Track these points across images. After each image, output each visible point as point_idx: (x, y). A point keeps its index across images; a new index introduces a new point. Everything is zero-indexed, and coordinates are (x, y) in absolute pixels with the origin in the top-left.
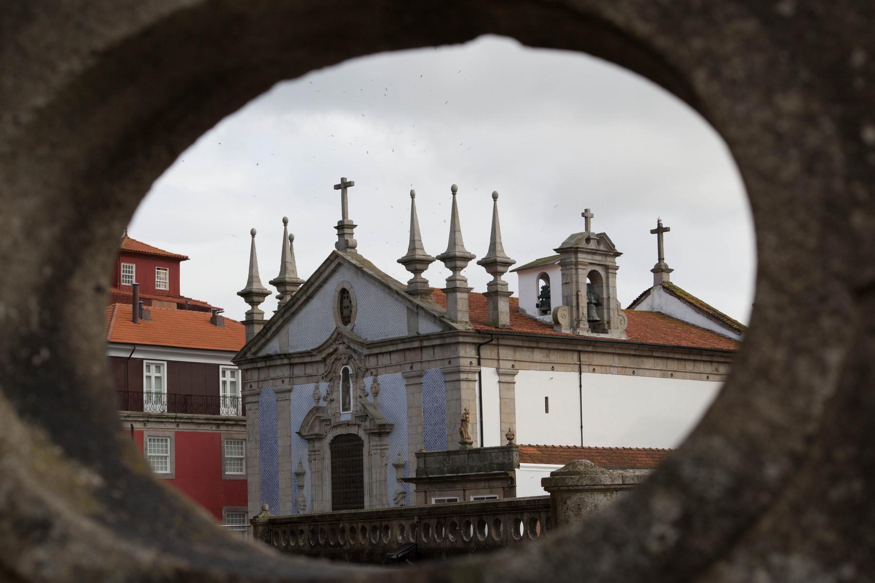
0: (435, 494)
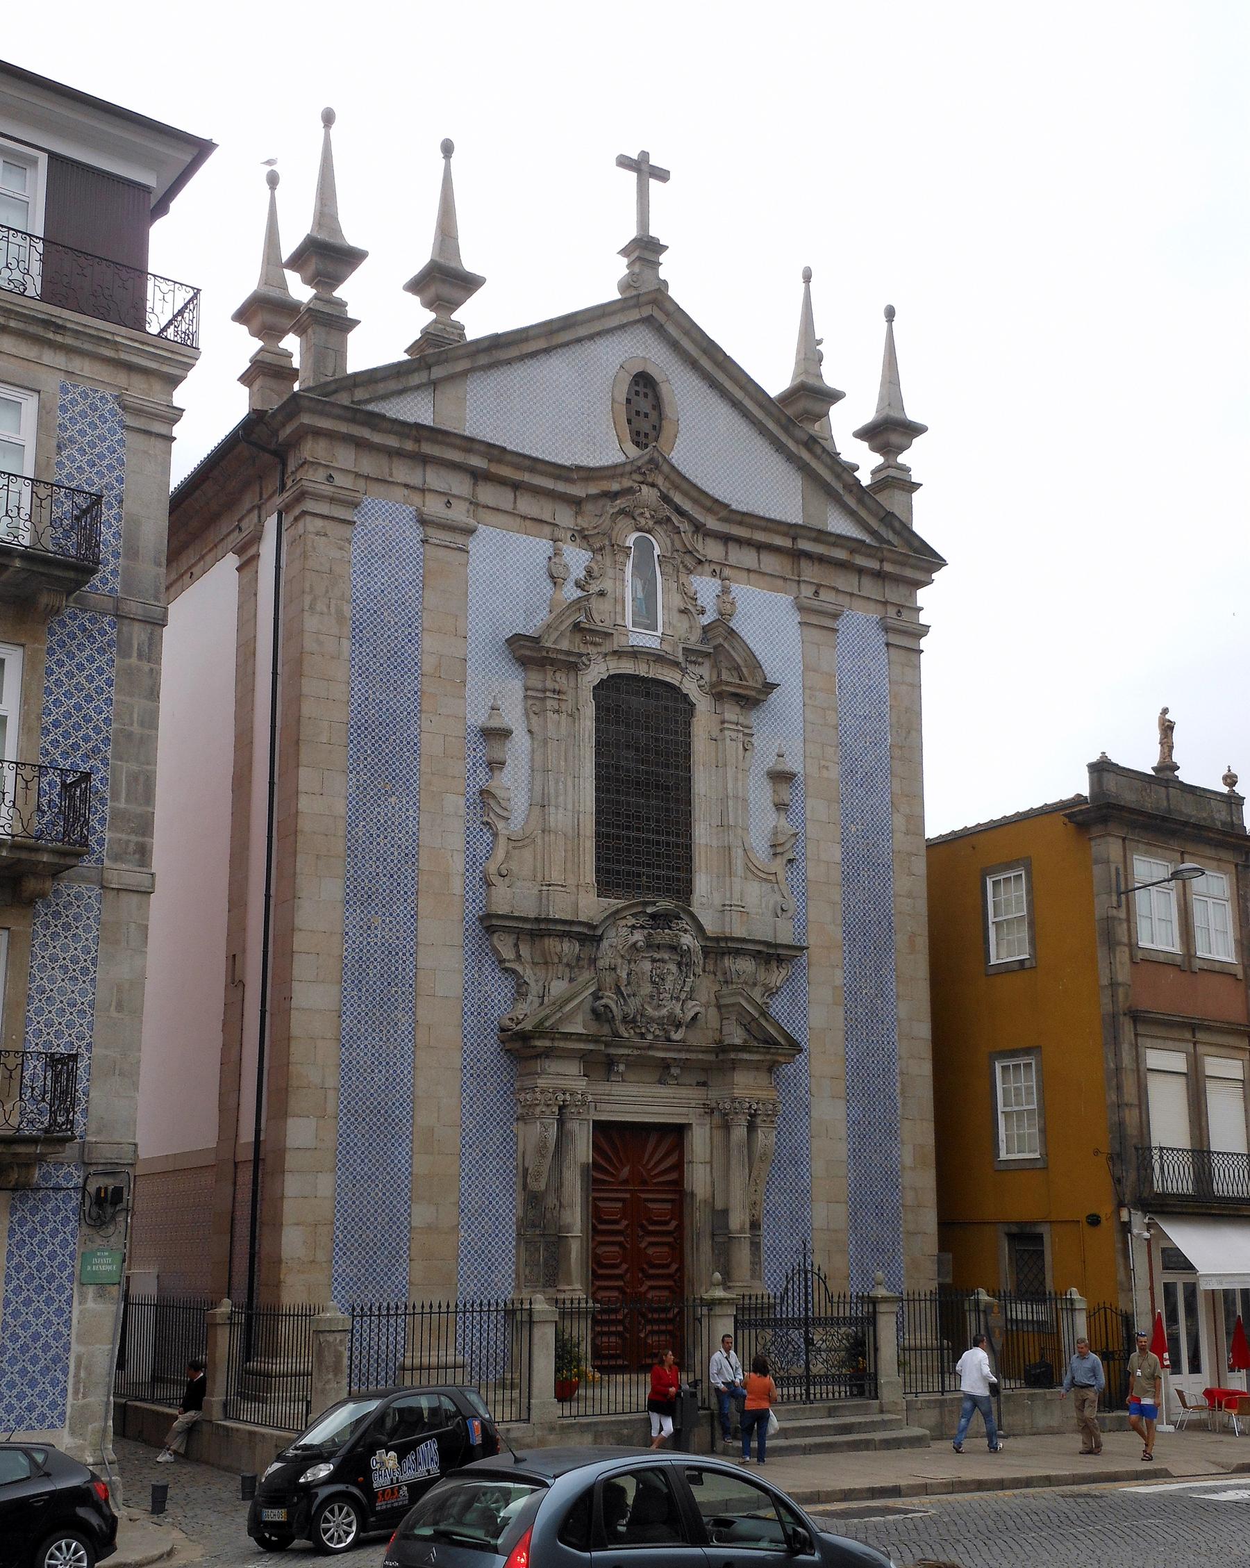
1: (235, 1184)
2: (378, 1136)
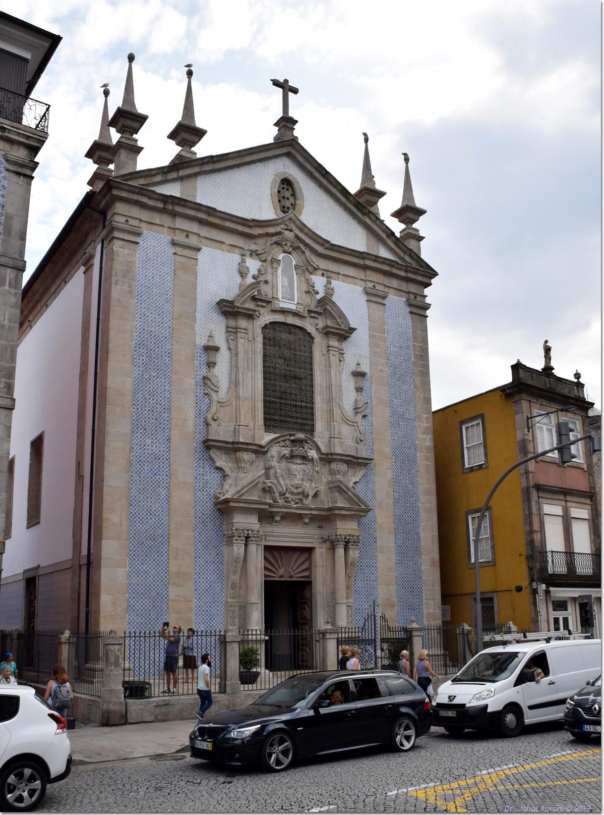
1: (80, 576)
2: (150, 551)
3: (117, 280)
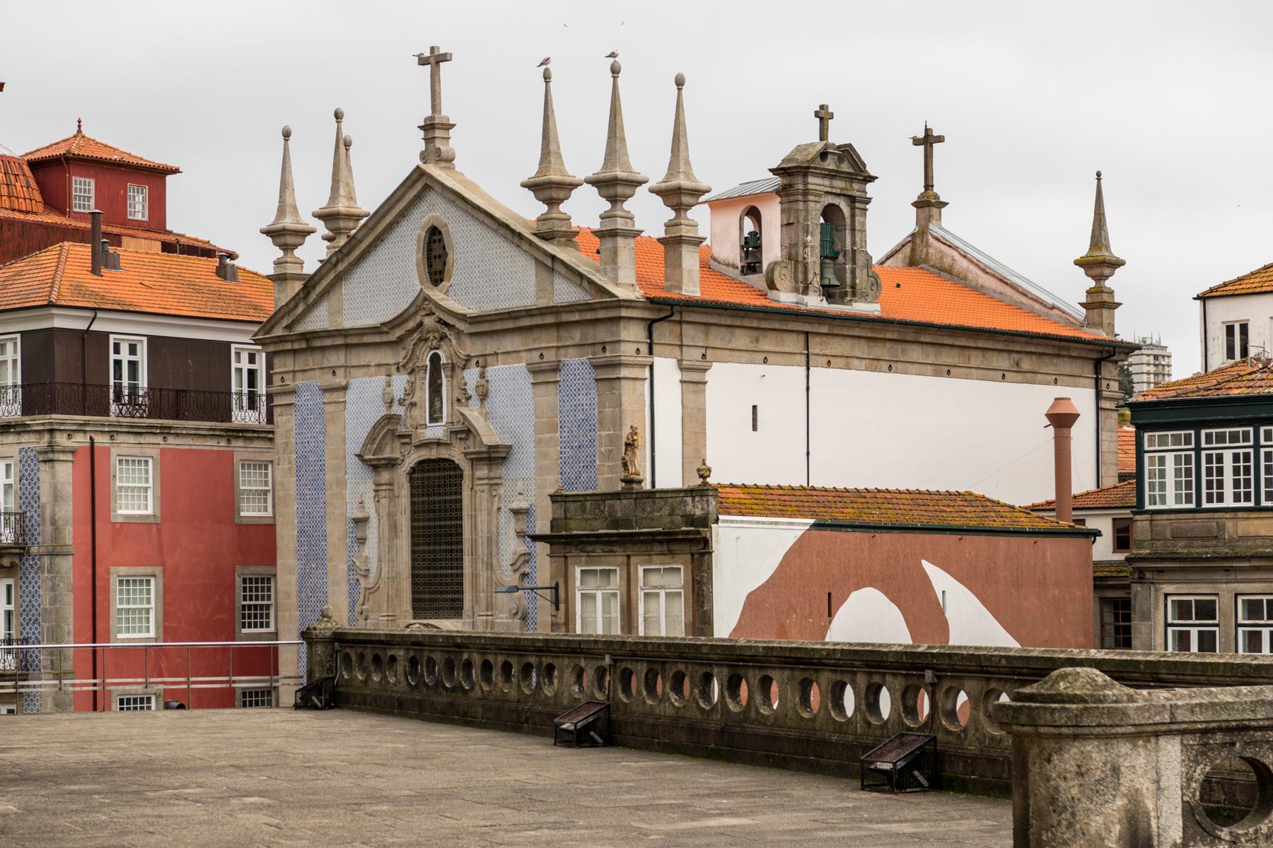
0: (581, 561)
3: (279, 458)
